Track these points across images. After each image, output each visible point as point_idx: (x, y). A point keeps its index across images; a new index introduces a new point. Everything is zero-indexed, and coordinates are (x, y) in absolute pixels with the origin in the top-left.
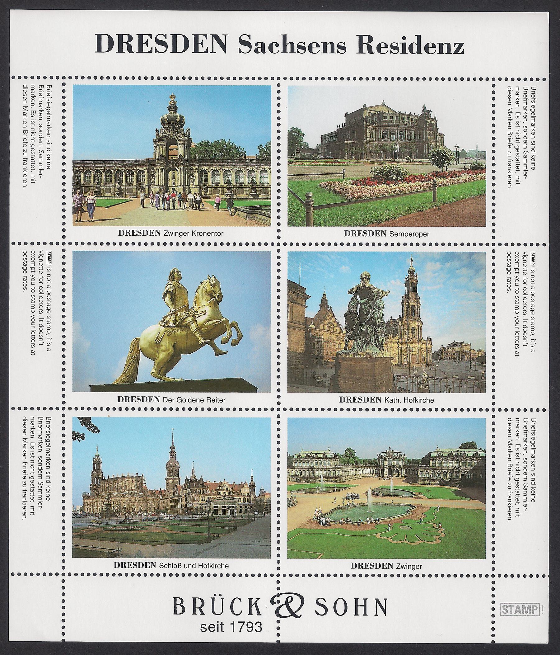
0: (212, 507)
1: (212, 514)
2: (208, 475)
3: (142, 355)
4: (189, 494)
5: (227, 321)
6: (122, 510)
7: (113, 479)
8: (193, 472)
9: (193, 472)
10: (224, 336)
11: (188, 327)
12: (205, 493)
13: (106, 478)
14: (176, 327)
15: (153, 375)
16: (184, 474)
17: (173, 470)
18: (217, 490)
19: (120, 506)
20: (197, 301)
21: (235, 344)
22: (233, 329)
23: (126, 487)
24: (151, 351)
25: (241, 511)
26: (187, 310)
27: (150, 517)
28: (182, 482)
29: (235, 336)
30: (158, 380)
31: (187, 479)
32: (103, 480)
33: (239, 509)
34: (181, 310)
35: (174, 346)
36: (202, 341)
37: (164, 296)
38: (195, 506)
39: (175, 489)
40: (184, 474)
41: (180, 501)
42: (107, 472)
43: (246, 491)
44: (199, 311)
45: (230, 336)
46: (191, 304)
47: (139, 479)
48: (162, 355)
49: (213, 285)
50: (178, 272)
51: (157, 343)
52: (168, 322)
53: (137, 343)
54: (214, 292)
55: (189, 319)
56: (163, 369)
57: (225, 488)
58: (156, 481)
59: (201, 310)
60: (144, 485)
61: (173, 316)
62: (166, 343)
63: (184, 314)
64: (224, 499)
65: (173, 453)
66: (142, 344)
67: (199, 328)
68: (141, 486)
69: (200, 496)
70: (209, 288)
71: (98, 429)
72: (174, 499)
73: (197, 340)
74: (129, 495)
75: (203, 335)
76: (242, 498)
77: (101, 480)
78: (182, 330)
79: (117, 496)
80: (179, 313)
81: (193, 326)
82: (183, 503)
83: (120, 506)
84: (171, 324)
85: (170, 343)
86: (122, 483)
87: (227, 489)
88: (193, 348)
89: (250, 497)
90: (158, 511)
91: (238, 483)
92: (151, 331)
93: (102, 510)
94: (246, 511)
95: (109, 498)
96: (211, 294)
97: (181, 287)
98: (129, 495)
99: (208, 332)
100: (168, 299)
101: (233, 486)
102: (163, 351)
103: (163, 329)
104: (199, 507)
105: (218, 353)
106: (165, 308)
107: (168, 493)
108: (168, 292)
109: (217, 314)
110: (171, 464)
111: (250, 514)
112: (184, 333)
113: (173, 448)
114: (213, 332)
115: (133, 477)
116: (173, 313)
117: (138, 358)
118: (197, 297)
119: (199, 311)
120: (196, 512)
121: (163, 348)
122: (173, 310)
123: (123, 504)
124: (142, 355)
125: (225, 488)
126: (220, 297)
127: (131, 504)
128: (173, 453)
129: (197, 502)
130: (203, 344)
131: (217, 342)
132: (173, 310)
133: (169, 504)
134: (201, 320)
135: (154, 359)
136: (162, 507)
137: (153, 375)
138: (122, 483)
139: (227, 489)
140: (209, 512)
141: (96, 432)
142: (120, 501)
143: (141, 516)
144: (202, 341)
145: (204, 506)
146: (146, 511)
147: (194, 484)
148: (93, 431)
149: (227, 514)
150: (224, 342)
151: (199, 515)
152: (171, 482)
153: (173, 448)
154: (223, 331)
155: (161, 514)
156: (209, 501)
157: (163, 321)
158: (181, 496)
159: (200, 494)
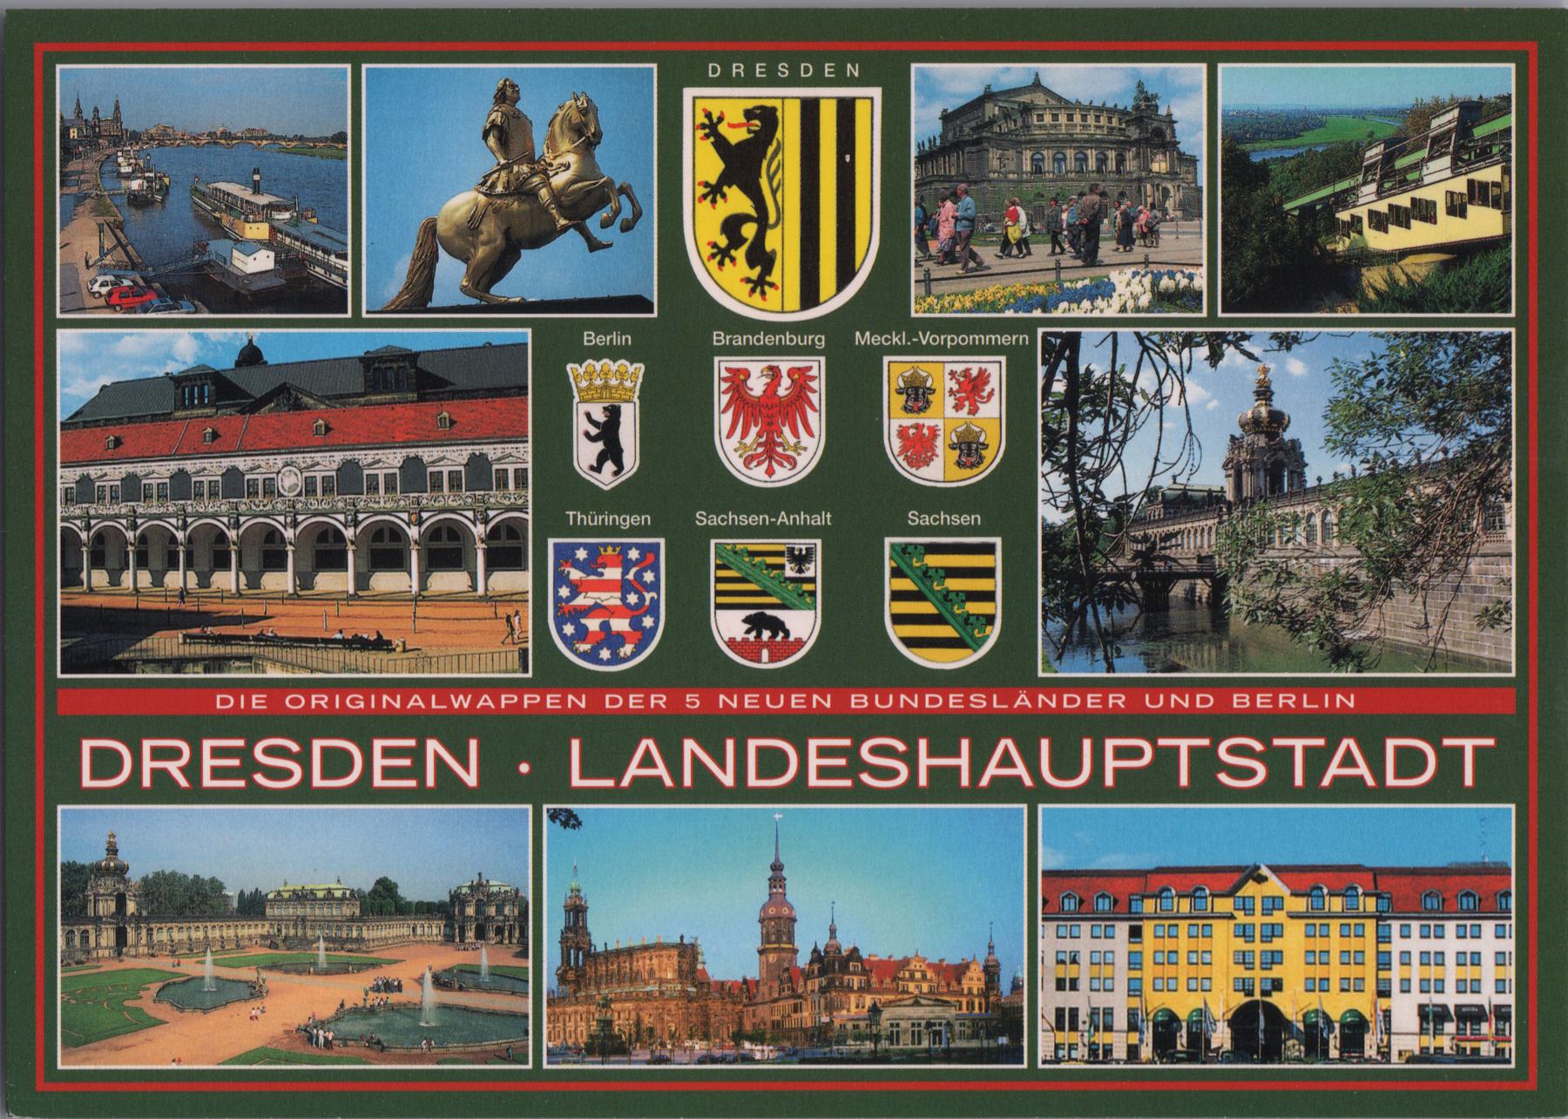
0: (885, 1024)
1: (884, 1044)
2: (877, 940)
3: (442, 253)
4: (823, 990)
5: (610, 183)
6: (643, 1035)
7: (618, 953)
8: (833, 932)
9: (833, 932)
10: (604, 213)
11: (533, 194)
12: (866, 989)
13: (600, 949)
15: (464, 289)
16: (807, 940)
17: (778, 927)
18: (895, 979)
19: (638, 1023)
20: (552, 144)
21: (627, 227)
22: (624, 199)
23: (651, 972)
24: (458, 242)
25: (962, 1035)
26: (531, 160)
27: (717, 1053)
28: (803, 960)
29: (627, 212)
31: (815, 951)
32: (591, 956)
33: (957, 1028)
34: (519, 162)
35: (507, 234)
36: (563, 222)
37: (485, 136)
38: (837, 1024)
39: (785, 976)
40: (807, 940)
41: (796, 1009)
42: (604, 933)
43: (974, 981)
44: (556, 163)
45: (617, 212)
46: (540, 148)
47: (687, 953)
48: (481, 252)
49: (584, 112)
50: (513, 86)
51: (471, 227)
52: (493, 185)
53: (430, 229)
54: (586, 125)
55: (536, 180)
56: (485, 281)
57: (918, 975)
58: (733, 957)
60: (699, 967)
61: (503, 174)
62: (489, 228)
63: (525, 168)
64: (917, 1003)
65: (777, 878)
66: (442, 227)
67: (556, 196)
68: (693, 970)
69: (853, 998)
70: (576, 118)
71: (576, 818)
72: (781, 1003)
73: (553, 221)
74: (662, 993)
75: (565, 210)
76: (964, 1001)
77: (588, 955)
78: (520, 200)
79: (628, 998)
80: (516, 168)
81: (544, 192)
82: (806, 1014)
83: (638, 1023)
84: (499, 189)
85: (497, 226)
86: (642, 964)
89: (987, 998)
90: (738, 1037)
91: (953, 959)
92: (461, 203)
93: (591, 1036)
94: (975, 1036)
95: (606, 1004)
96: (579, 130)
97: (518, 116)
98: (662, 993)
99: (574, 205)
100: (492, 141)
101: (938, 968)
102: (484, 244)
103: (482, 198)
104: (849, 1026)
105: (594, 245)
106: (487, 158)
107: (764, 989)
108: (493, 125)
109: (589, 167)
110: (772, 911)
111: (985, 1044)
112: (526, 207)
113: (777, 867)
114: (582, 204)
115: (674, 946)
116: (503, 167)
117: (435, 257)
118: (552, 137)
119: (556, 163)
120: (841, 1040)
121: (483, 237)
122: (503, 161)
123: (647, 1021)
124: (442, 253)
125: (918, 975)
126: (598, 135)
127: (666, 1018)
128: (777, 878)
129: (844, 1012)
130: (565, 229)
131: (593, 224)
132: (503, 161)
133: (768, 1019)
134: (559, 180)
135: (466, 260)
136: (748, 1027)
137: (464, 289)
138: (642, 964)
140: (876, 1038)
141: (574, 827)
142: (638, 1010)
143: (692, 1049)
144: (563, 222)
145: (862, 1024)
146: (706, 1037)
147: (834, 965)
148: (565, 824)
149: (925, 1044)
150: (606, 224)
151: (852, 1045)
152: (772, 958)
153: (777, 867)
154: (603, 201)
155: (747, 1045)
156: (875, 1010)
157: (483, 184)
158: (800, 997)
159: (850, 989)
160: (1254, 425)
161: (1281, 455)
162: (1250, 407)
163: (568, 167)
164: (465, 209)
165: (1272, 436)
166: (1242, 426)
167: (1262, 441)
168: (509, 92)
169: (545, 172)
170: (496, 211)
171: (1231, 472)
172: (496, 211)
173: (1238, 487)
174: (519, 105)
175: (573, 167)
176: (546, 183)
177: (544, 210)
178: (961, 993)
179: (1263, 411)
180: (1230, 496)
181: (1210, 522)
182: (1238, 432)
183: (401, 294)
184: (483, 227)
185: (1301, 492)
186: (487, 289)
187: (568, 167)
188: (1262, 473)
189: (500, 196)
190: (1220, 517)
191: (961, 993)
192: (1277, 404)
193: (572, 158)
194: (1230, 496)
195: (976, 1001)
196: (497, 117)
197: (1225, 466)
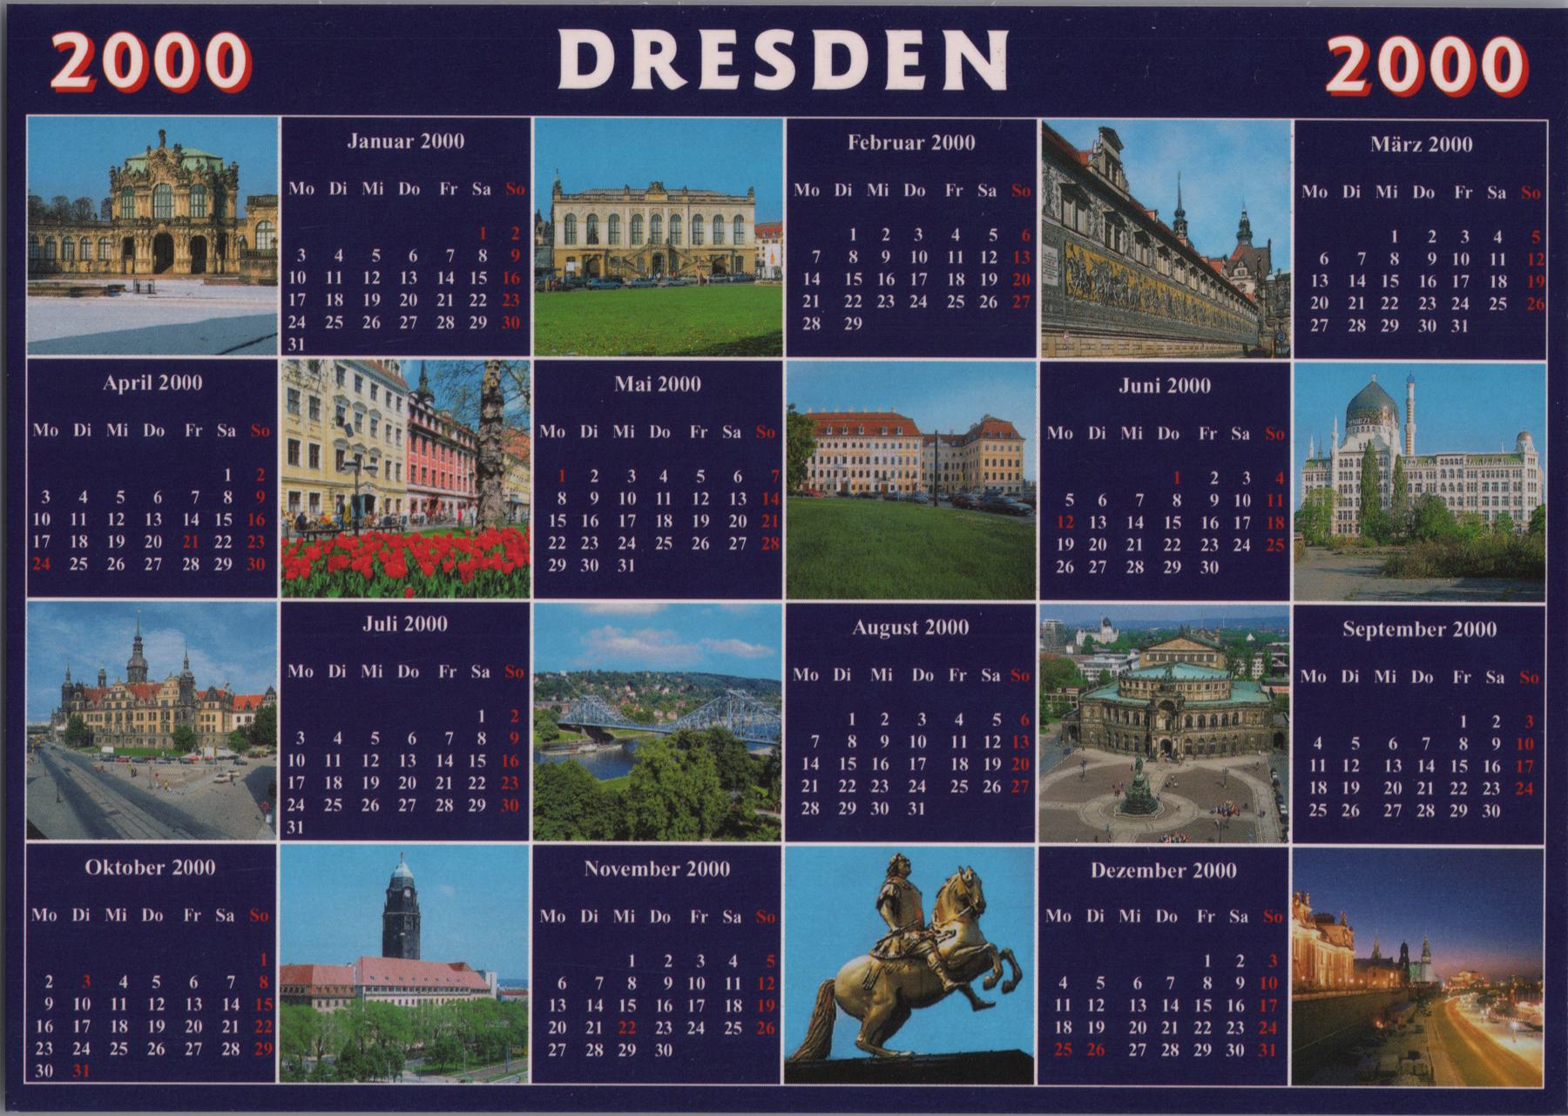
3: (840, 1012)
10: (987, 976)
11: (923, 958)
14: (902, 958)
21: (1008, 988)
22: (1005, 963)
24: (854, 1002)
26: (921, 927)
29: (1008, 974)
30: (867, 1055)
35: (899, 993)
36: (949, 983)
37: (879, 905)
44: (943, 930)
45: (1000, 974)
46: (929, 917)
48: (875, 1011)
49: (969, 884)
50: (905, 860)
51: (865, 989)
52: (886, 950)
53: (829, 990)
55: (925, 945)
56: (878, 1036)
59: (946, 928)
62: (882, 989)
63: (915, 935)
67: (943, 960)
70: (961, 890)
73: (940, 982)
75: (951, 974)
78: (910, 964)
81: (931, 957)
84: (892, 953)
87: (123, 696)
88: (932, 996)
92: (857, 967)
96: (964, 900)
97: (909, 887)
99: (961, 968)
100: (885, 910)
102: (878, 1003)
103: (876, 963)
105: (978, 1005)
106: (881, 925)
108: (886, 896)
112: (915, 969)
117: (833, 1015)
119: (943, 930)
121: (876, 998)
124: (840, 1012)
126: (982, 906)
130: (951, 990)
131: (977, 985)
132: (895, 929)
134: (946, 946)
135: (860, 1017)
137: (858, 1044)
139: (123, 696)
144: (949, 983)
150: (988, 986)
157: (877, 949)
163: (954, 934)
164: (862, 970)
168: (901, 865)
169: (933, 939)
170: (889, 973)
172: (889, 973)
174: (910, 878)
175: (959, 934)
176: (934, 948)
177: (932, 973)
178: (156, 707)
183: (802, 1048)
184: (876, 989)
186: (880, 1043)
187: (954, 934)
189: (892, 960)
191: (156, 707)
193: (958, 927)
195: (172, 712)
196: (890, 889)
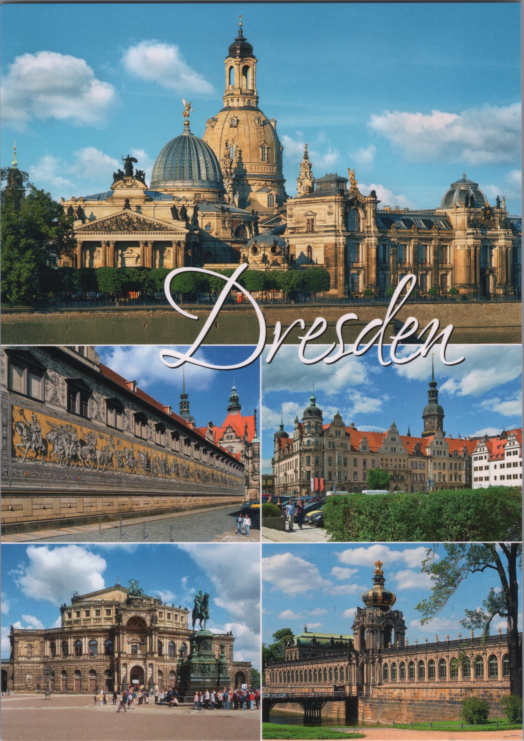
160: (373, 601)
161: (390, 622)
162: (370, 589)
165: (385, 608)
166: (364, 601)
167: (379, 613)
171: (358, 631)
173: (363, 643)
179: (379, 592)
180: (357, 647)
181: (342, 664)
182: (363, 606)
185: (404, 649)
188: (379, 634)
190: (350, 661)
192: (388, 587)
194: (357, 647)
197: (354, 627)
